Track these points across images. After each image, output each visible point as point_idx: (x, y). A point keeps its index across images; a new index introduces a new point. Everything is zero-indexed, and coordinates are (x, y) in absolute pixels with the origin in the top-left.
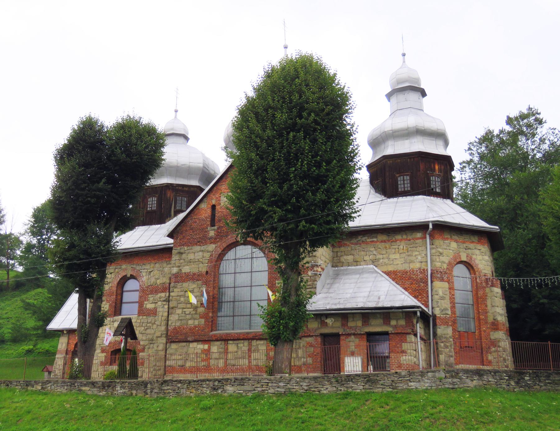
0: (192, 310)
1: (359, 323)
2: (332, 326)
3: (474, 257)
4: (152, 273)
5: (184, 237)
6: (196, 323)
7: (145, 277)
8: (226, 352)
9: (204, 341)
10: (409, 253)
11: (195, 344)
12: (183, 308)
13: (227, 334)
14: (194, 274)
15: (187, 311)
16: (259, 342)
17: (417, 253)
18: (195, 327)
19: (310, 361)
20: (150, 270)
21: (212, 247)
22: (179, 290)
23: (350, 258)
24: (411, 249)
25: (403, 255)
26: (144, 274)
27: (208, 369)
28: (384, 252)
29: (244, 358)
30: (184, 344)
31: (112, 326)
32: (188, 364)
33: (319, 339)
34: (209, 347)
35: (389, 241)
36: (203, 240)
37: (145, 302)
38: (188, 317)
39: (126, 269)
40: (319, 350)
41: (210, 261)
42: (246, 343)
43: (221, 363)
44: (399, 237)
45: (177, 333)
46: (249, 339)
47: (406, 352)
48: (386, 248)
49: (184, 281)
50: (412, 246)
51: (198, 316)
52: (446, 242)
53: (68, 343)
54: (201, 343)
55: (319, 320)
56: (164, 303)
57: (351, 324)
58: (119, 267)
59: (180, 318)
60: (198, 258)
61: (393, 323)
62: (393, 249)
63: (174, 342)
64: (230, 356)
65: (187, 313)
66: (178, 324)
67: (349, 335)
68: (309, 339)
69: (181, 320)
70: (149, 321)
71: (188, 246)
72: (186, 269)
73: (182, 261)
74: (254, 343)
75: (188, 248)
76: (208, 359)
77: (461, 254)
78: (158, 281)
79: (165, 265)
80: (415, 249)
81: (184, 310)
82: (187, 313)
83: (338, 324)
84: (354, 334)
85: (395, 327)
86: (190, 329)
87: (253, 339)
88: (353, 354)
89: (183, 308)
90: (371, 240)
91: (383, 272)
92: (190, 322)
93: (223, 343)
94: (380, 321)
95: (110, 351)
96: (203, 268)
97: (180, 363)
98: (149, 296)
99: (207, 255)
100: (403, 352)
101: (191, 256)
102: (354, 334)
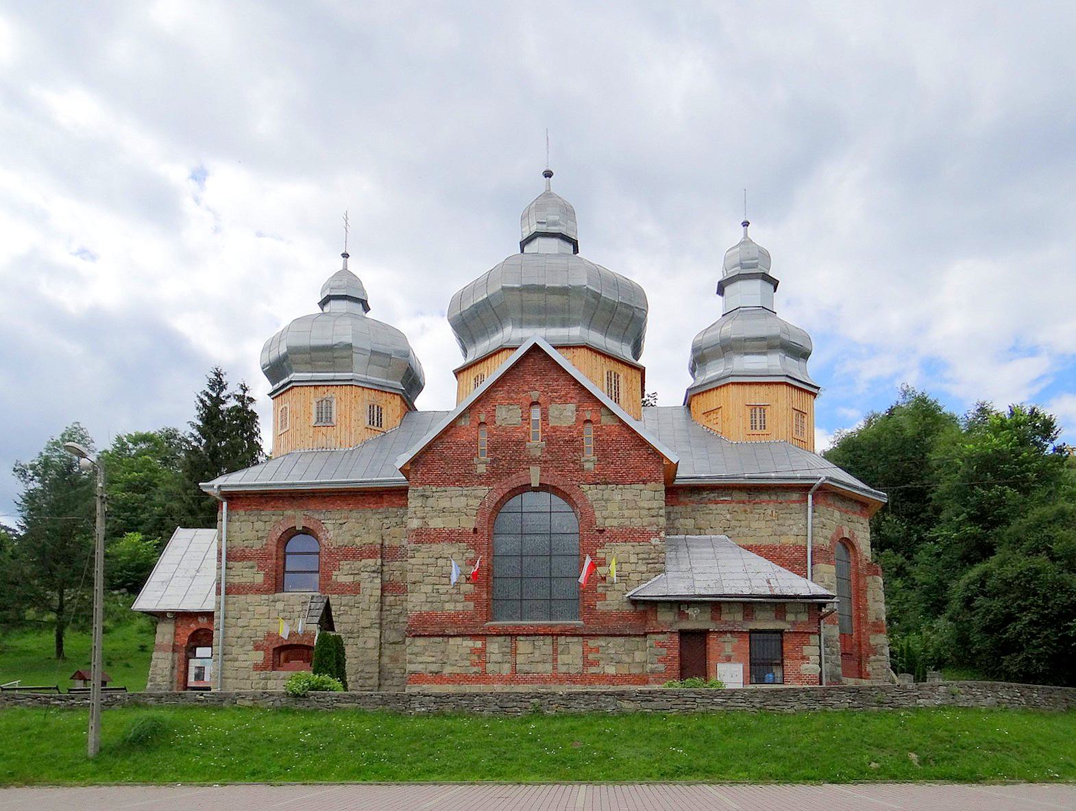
1: (739, 617)
2: (696, 620)
3: (856, 532)
4: (344, 526)
6: (460, 607)
7: (332, 533)
8: (514, 652)
9: (475, 636)
10: (781, 522)
11: (459, 640)
12: (434, 584)
13: (516, 626)
14: (452, 532)
15: (443, 589)
16: (569, 639)
17: (792, 522)
18: (458, 614)
19: (661, 667)
20: (341, 522)
23: (690, 523)
24: (784, 515)
27: (483, 677)
29: (544, 662)
32: (447, 670)
33: (676, 638)
34: (484, 645)
37: (335, 573)
39: (294, 517)
40: (676, 653)
41: (480, 512)
42: (549, 640)
43: (506, 669)
46: (552, 635)
47: (808, 659)
48: (745, 511)
49: (433, 541)
50: (784, 511)
51: (461, 597)
53: (175, 634)
55: (676, 610)
56: (375, 575)
60: (459, 505)
61: (790, 617)
62: (756, 513)
63: (420, 636)
64: (520, 659)
65: (441, 591)
66: (426, 608)
69: (432, 602)
72: (436, 523)
74: (562, 640)
77: (843, 527)
78: (357, 540)
79: (369, 515)
80: (788, 516)
81: (436, 587)
83: (707, 616)
84: (731, 632)
85: (794, 623)
86: (449, 616)
87: (558, 635)
88: (728, 659)
96: (469, 524)
97: (434, 668)
98: (341, 563)
100: (803, 658)
101: (444, 503)
102: (731, 632)
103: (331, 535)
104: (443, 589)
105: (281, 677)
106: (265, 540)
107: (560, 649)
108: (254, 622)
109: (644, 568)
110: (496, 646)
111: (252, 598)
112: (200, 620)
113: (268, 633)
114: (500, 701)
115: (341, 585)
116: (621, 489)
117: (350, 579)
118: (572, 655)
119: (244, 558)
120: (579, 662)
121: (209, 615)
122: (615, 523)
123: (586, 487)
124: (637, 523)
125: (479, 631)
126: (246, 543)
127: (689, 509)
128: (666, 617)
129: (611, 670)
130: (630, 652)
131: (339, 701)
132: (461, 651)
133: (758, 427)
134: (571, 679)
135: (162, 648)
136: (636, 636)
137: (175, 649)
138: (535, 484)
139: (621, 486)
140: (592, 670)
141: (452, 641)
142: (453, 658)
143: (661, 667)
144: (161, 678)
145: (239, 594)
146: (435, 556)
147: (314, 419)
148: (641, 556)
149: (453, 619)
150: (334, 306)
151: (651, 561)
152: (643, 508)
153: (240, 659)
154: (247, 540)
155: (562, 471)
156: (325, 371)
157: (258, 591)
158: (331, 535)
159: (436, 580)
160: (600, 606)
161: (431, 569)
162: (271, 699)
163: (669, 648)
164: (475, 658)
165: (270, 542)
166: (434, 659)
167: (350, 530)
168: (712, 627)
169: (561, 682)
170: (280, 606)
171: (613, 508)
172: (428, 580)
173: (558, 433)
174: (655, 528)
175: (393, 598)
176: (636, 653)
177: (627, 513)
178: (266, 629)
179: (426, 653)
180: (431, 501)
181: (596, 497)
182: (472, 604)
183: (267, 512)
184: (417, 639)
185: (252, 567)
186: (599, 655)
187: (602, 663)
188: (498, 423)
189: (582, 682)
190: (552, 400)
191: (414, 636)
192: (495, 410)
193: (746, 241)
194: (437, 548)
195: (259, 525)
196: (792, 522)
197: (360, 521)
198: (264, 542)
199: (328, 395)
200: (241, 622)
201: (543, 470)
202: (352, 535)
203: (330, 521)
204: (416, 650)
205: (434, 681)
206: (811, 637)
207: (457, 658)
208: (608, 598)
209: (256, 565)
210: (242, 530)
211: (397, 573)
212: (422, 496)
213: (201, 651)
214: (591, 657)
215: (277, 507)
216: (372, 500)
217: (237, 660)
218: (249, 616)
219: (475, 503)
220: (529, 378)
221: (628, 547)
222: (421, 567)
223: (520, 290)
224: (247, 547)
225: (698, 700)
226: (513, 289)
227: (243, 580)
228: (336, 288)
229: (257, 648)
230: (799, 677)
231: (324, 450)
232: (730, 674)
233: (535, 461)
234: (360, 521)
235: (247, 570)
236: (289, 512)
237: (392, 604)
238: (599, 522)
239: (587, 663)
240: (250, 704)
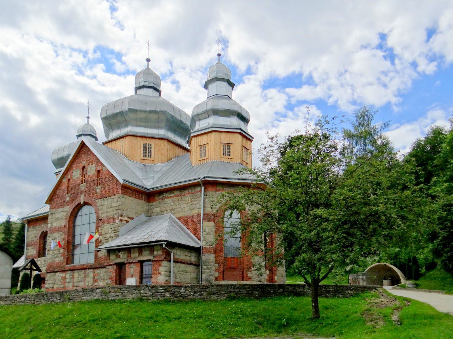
8: (73, 278)
11: (58, 273)
23: (158, 209)
24: (194, 200)
25: (189, 205)
28: (177, 204)
30: (53, 274)
33: (115, 267)
34: (65, 275)
35: (181, 195)
42: (83, 271)
44: (186, 192)
46: (84, 269)
47: (161, 274)
50: (194, 197)
52: (218, 192)
57: (132, 255)
59: (52, 257)
64: (75, 280)
65: (55, 253)
67: (130, 263)
74: (87, 271)
81: (54, 251)
84: (134, 263)
87: (86, 269)
88: (132, 276)
90: (170, 195)
91: (177, 218)
92: (57, 259)
94: (147, 252)
99: (65, 214)
100: (159, 273)
120: (92, 281)
123: (97, 201)
127: (158, 203)
133: (147, 156)
164: (62, 281)
185: (33, 248)
195: (35, 232)
201: (85, 195)
227: (31, 254)
239: (95, 281)
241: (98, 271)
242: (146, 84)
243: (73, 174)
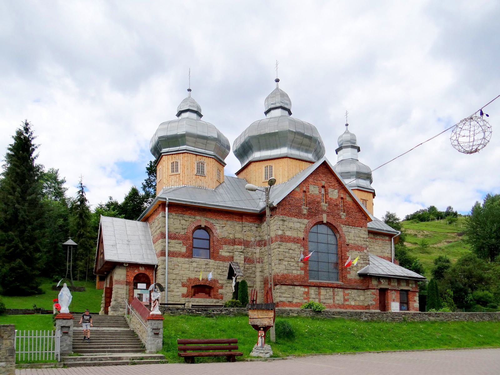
0: (295, 263)
1: (396, 284)
2: (384, 285)
4: (224, 228)
5: (284, 209)
6: (299, 273)
8: (319, 294)
9: (305, 286)
10: (383, 247)
11: (299, 287)
12: (289, 261)
13: (320, 283)
14: (295, 238)
15: (292, 264)
16: (339, 290)
17: (387, 248)
18: (298, 276)
19: (374, 303)
21: (306, 221)
22: (284, 248)
26: (218, 228)
29: (330, 299)
30: (291, 287)
31: (191, 265)
32: (295, 301)
33: (378, 291)
34: (308, 290)
35: (374, 238)
36: (299, 215)
37: (221, 251)
38: (293, 268)
42: (332, 289)
44: (378, 237)
45: (285, 278)
49: (287, 242)
51: (299, 268)
53: (127, 275)
54: (303, 287)
55: (378, 280)
56: (241, 253)
57: (392, 284)
58: (194, 217)
59: (287, 268)
63: (283, 285)
64: (322, 297)
65: (291, 265)
66: (285, 272)
68: (373, 291)
69: (288, 269)
70: (225, 265)
71: (289, 216)
72: (288, 233)
73: (285, 227)
75: (289, 218)
76: (308, 298)
79: (236, 224)
81: (289, 263)
82: (291, 265)
83: (387, 283)
84: (395, 290)
86: (294, 276)
87: (335, 288)
88: (394, 301)
89: (289, 261)
93: (317, 288)
94: (405, 284)
95: (191, 286)
96: (301, 236)
97: (290, 300)
98: (224, 246)
100: (415, 301)
101: (291, 225)
102: (395, 290)
103: (218, 231)
104: (292, 264)
105: (196, 301)
106: (186, 230)
107: (335, 294)
108: (182, 272)
109: (362, 262)
110: (313, 291)
111: (180, 259)
112: (140, 268)
113: (189, 278)
114: (393, 316)
115: (223, 257)
116: (354, 228)
117: (227, 254)
118: (340, 295)
119: (175, 238)
120: (342, 299)
121: (152, 268)
122: (353, 242)
123: (342, 226)
124: (360, 243)
125: (306, 284)
126: (177, 231)
128: (374, 282)
129: (353, 303)
130: (359, 296)
131: (334, 315)
132: (300, 292)
134: (340, 306)
135: (118, 282)
136: (361, 289)
137: (128, 283)
138: (325, 222)
139: (354, 227)
140: (347, 303)
141: (296, 288)
142: (297, 295)
143: (374, 303)
144: (122, 300)
145: (174, 257)
146: (289, 248)
147: (195, 172)
148: (362, 257)
149: (296, 278)
150: (184, 115)
151: (365, 259)
152: (362, 238)
153: (175, 291)
154: (177, 229)
155: (334, 217)
156: (201, 148)
157: (183, 256)
158: (218, 231)
159: (289, 259)
160: (349, 276)
161: (287, 255)
162: (305, 313)
163: (376, 295)
164: (305, 296)
165: (189, 231)
166: (289, 296)
167: (227, 230)
168: (389, 287)
169: (336, 308)
170: (194, 265)
171: (352, 235)
172: (286, 259)
173: (332, 201)
174: (365, 246)
175: (248, 265)
176: (361, 296)
177: (357, 239)
178: (188, 276)
179: (286, 293)
180: (286, 223)
181: (346, 230)
182: (303, 272)
183: (187, 216)
184: (282, 286)
185: (180, 243)
186: (349, 297)
187: (350, 300)
188: (310, 192)
189: (343, 308)
190: (329, 187)
191: (281, 285)
192: (309, 186)
193: (347, 132)
194: (290, 245)
195: (183, 222)
196: (387, 248)
197: (232, 226)
198: (186, 231)
199: (202, 160)
200: (175, 272)
201: (328, 216)
202: (228, 233)
203: (218, 225)
204: (282, 291)
205: (289, 306)
206: (417, 293)
207: (299, 296)
208: (351, 273)
209: (182, 242)
210: (175, 223)
211: (250, 254)
212: (282, 220)
213: (140, 286)
214: (346, 297)
215: (192, 214)
216: (237, 217)
217: (173, 291)
218: (179, 269)
219: (304, 226)
220: (321, 175)
221: (356, 253)
222: (283, 253)
223: (295, 133)
224: (177, 233)
225: (452, 317)
226: (292, 132)
228: (191, 106)
229: (183, 286)
230: (414, 308)
231: (201, 188)
232: (395, 307)
233: (324, 211)
234: (232, 226)
235: (177, 244)
236: (198, 218)
237: (248, 268)
238: (347, 241)
239: (345, 300)
240: (295, 315)
241: (347, 292)
242: (283, 105)
243: (310, 188)
